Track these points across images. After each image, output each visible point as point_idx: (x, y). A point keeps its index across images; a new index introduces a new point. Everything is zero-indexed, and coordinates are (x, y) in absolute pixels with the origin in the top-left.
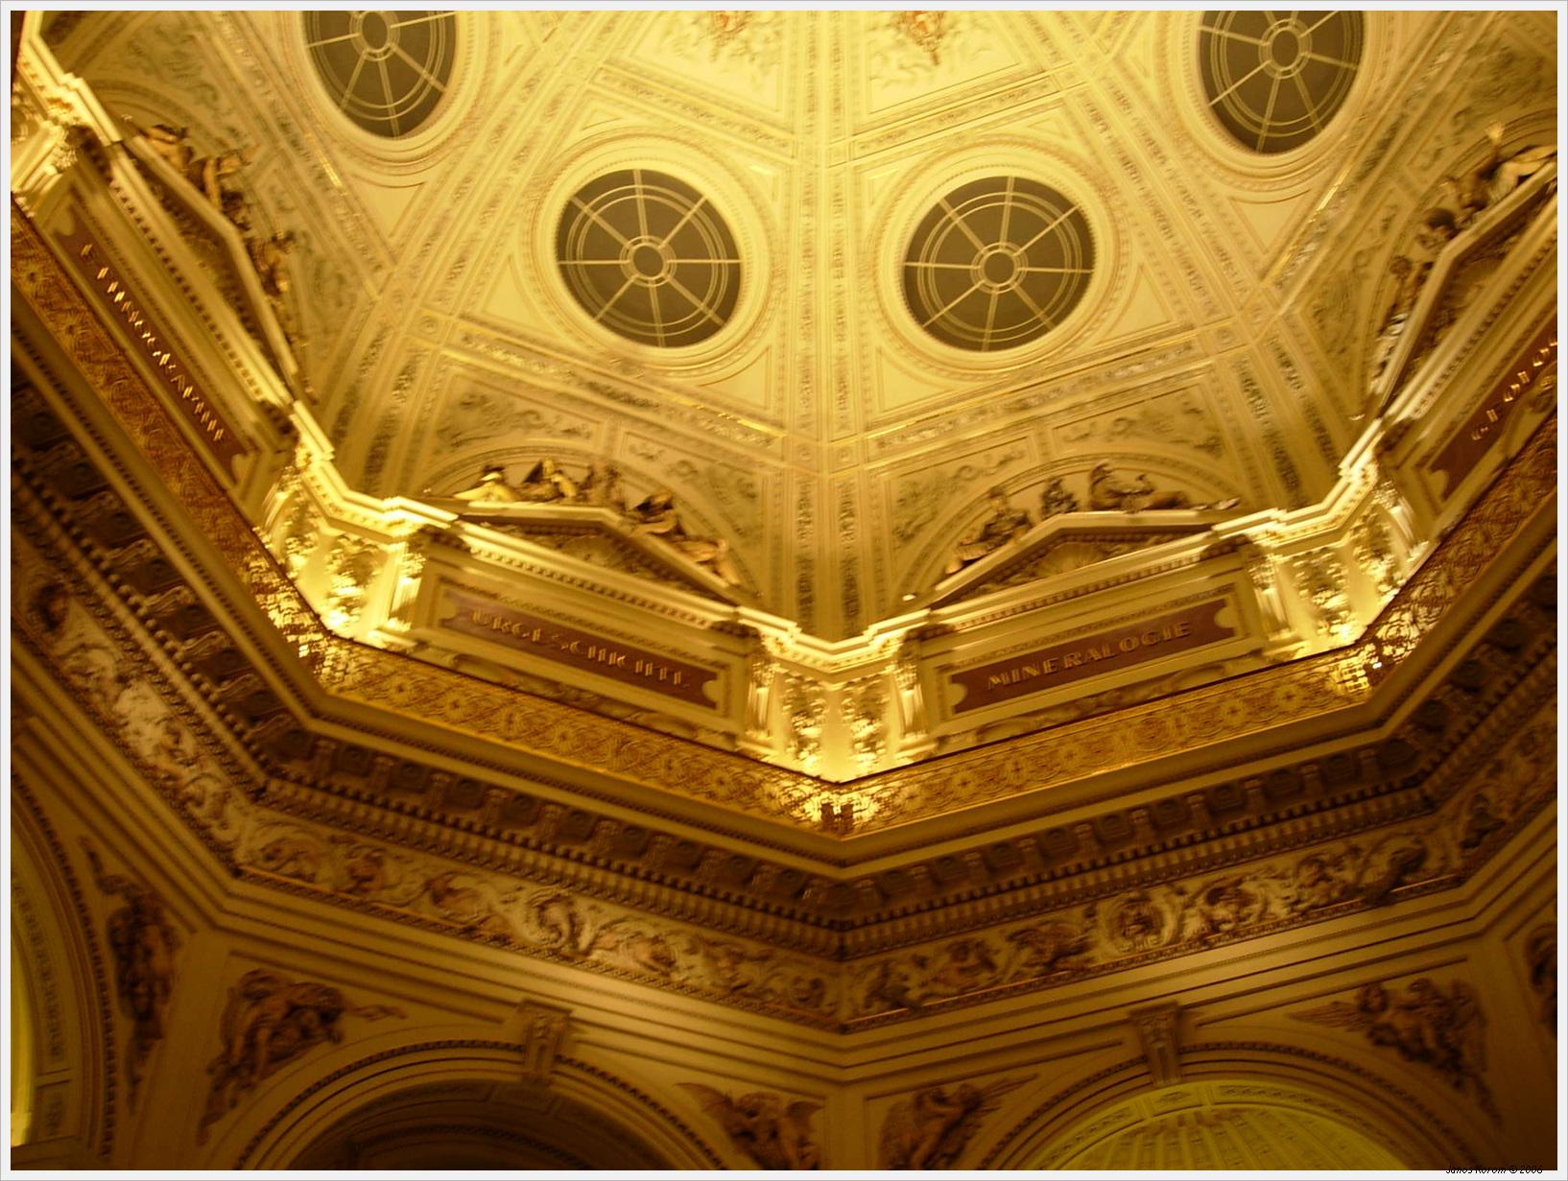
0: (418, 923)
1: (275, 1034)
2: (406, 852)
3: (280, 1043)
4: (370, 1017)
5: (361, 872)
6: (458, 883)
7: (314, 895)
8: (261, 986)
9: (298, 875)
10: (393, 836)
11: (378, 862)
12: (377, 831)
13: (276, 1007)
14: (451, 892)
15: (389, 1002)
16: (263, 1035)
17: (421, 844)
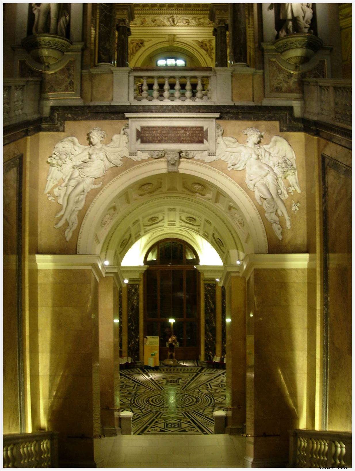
0: (152, 26)
1: (136, 48)
2: (148, 16)
3: (137, 49)
4: (148, 41)
5: (143, 21)
6: (156, 18)
7: (137, 26)
8: (133, 41)
9: (134, 24)
10: (146, 14)
11: (144, 19)
12: (144, 14)
13: (135, 44)
14: (155, 20)
15: (150, 39)
16: (134, 49)
17: (150, 14)
